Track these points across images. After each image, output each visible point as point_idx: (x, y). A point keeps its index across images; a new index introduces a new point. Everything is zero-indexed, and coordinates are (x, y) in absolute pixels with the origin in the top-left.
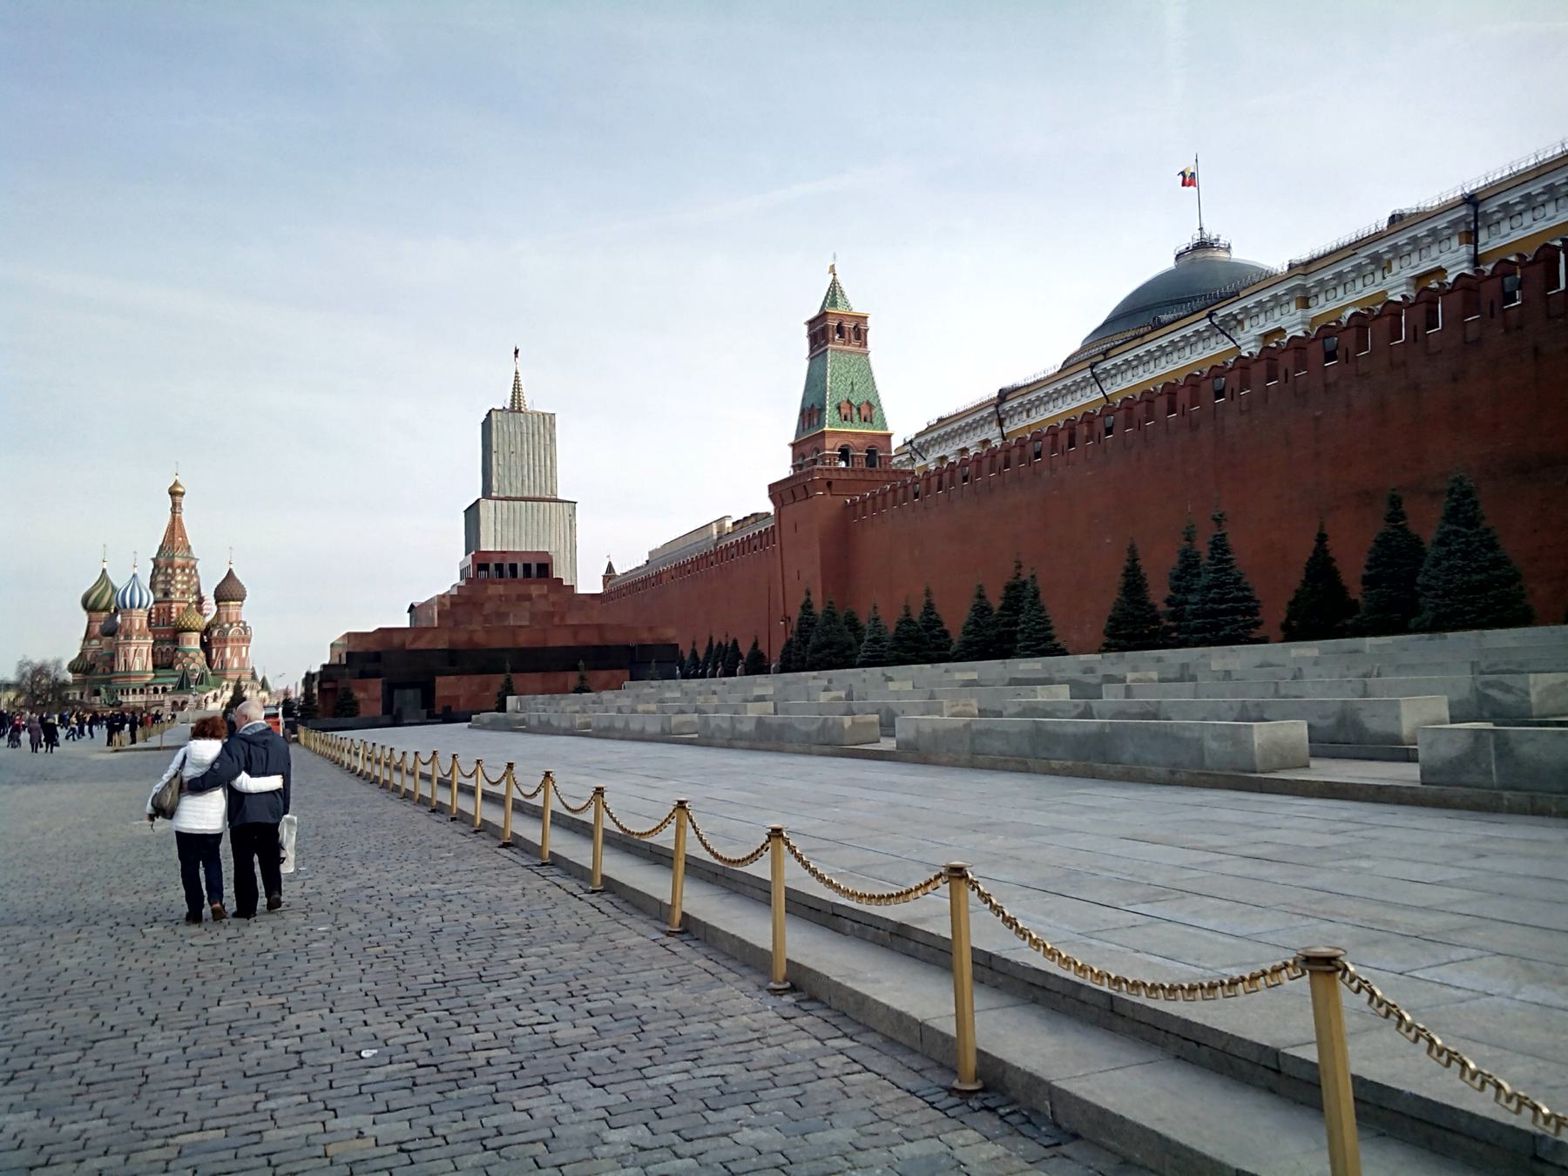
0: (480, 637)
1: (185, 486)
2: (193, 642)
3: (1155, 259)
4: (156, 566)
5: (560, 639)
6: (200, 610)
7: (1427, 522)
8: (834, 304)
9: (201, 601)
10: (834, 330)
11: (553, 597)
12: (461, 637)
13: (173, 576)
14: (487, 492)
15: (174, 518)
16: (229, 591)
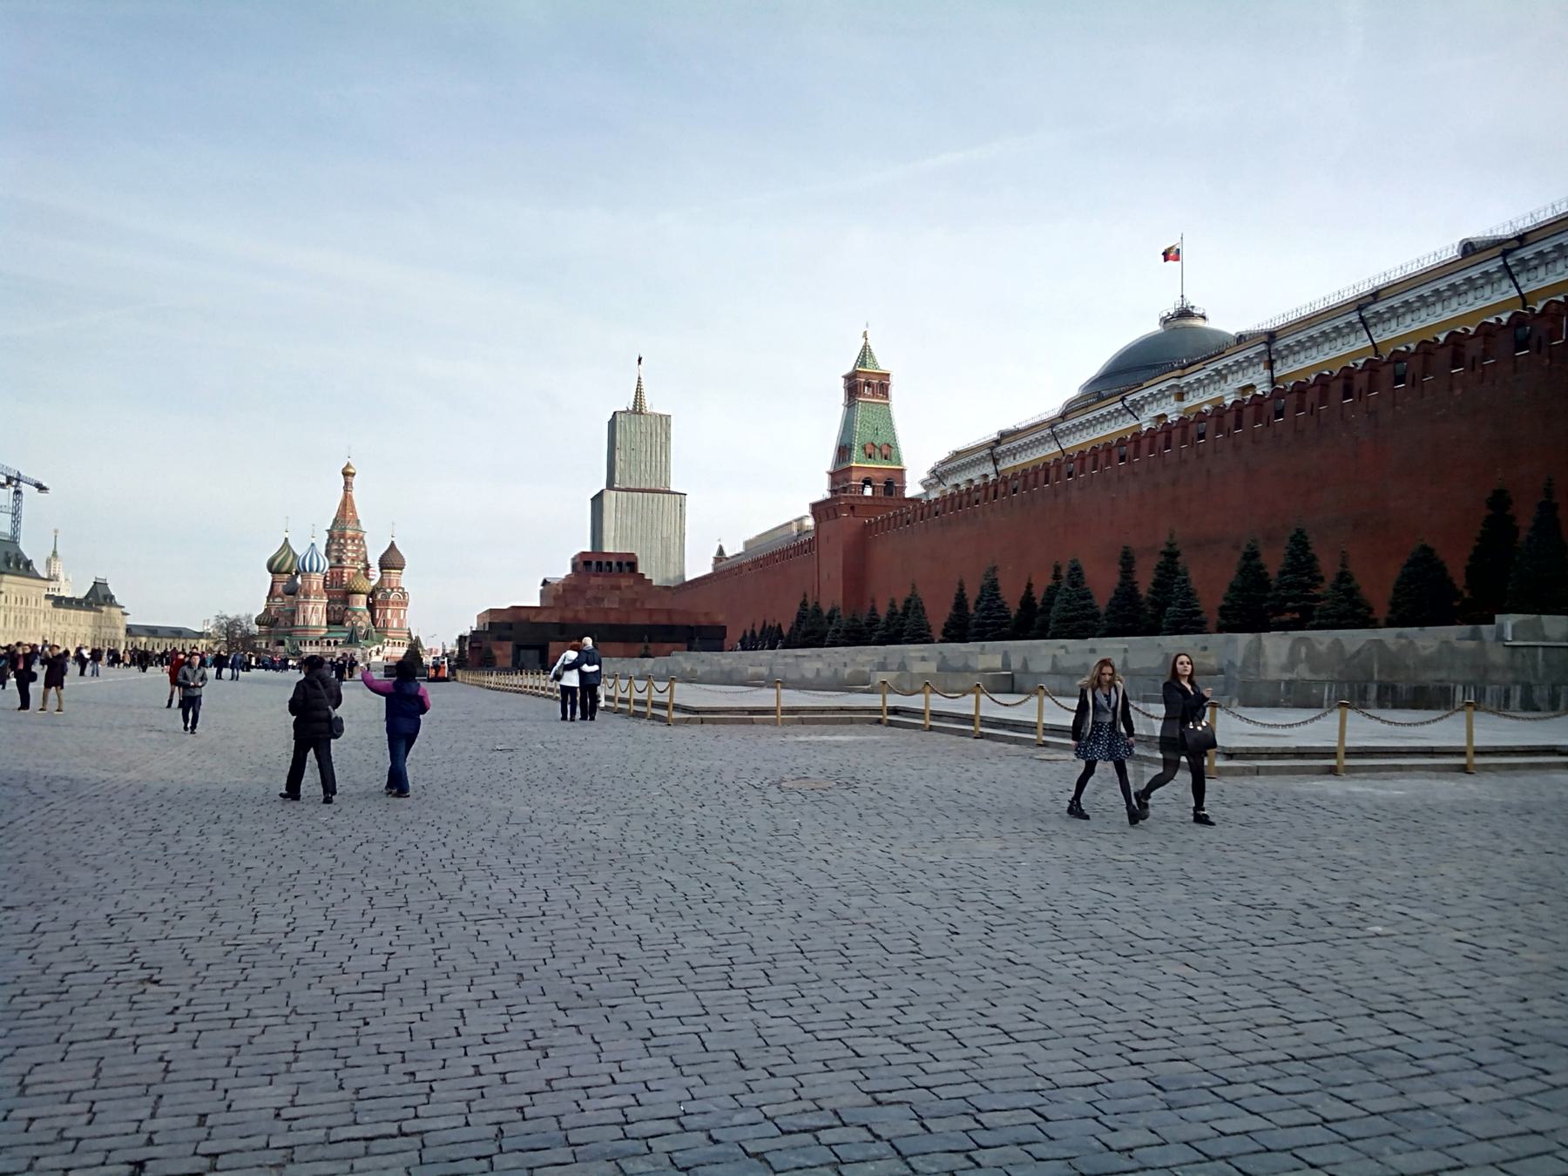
0: (582, 615)
1: (355, 468)
2: (360, 602)
3: (1141, 323)
4: (331, 537)
5: (639, 619)
6: (367, 575)
7: (1274, 562)
8: (864, 364)
9: (367, 567)
10: (865, 385)
11: (637, 588)
12: (569, 615)
13: (345, 545)
14: (610, 484)
15: (346, 496)
16: (391, 560)
